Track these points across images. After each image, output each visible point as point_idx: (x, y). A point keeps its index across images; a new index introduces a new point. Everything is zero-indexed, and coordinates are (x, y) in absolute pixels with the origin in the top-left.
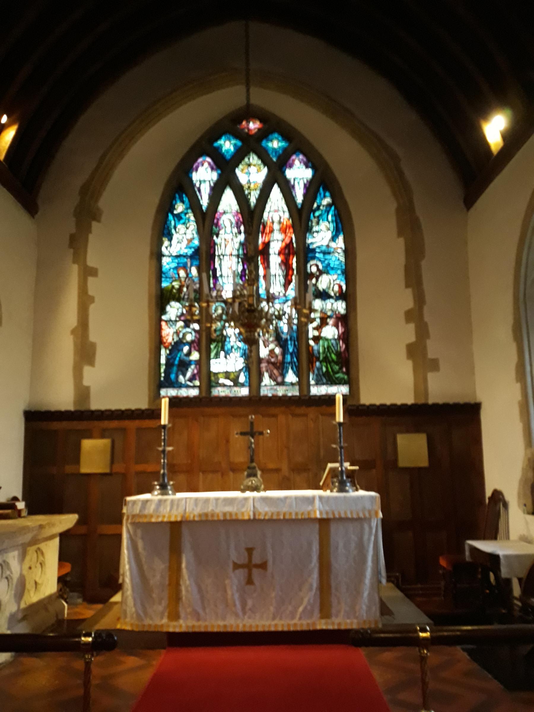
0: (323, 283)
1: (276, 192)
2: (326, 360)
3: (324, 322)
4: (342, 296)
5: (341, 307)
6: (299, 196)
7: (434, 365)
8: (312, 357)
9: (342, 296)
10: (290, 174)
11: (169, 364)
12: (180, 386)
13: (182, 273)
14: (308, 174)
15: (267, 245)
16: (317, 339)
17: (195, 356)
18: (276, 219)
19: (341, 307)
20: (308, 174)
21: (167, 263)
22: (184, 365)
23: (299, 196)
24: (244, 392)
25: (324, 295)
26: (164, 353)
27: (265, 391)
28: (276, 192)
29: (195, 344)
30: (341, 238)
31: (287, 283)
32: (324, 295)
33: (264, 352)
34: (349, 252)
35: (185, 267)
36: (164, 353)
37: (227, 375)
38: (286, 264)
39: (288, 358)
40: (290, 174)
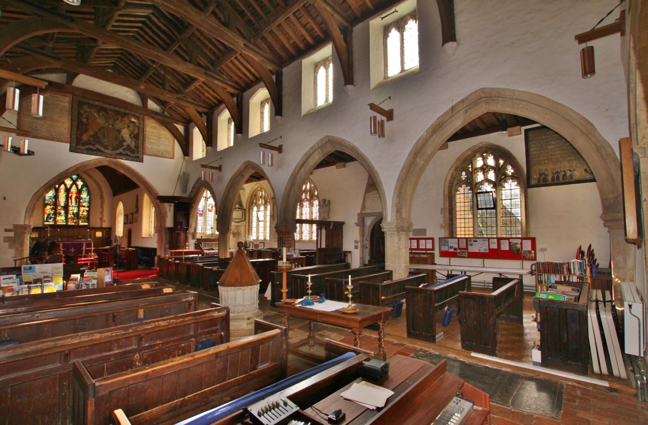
0: (84, 204)
1: (74, 186)
2: (84, 218)
3: (84, 211)
4: (88, 207)
5: (87, 209)
6: (80, 187)
7: (104, 221)
8: (81, 218)
9: (88, 207)
10: (78, 183)
11: (47, 218)
12: (49, 222)
13: (51, 200)
14: (82, 183)
15: (71, 196)
16: (82, 214)
17: (53, 216)
18: (74, 191)
19: (87, 209)
20: (82, 183)
21: (47, 198)
22: (51, 218)
23: (80, 187)
24: (65, 223)
25: (84, 207)
26: (46, 216)
27: (69, 224)
28: (74, 186)
29: (53, 214)
30: (88, 197)
31: (76, 204)
32: (84, 207)
33: (70, 216)
34: (90, 199)
35: (51, 199)
36: (46, 216)
37: (61, 220)
38: (76, 200)
39: (75, 217)
40: (78, 183)
